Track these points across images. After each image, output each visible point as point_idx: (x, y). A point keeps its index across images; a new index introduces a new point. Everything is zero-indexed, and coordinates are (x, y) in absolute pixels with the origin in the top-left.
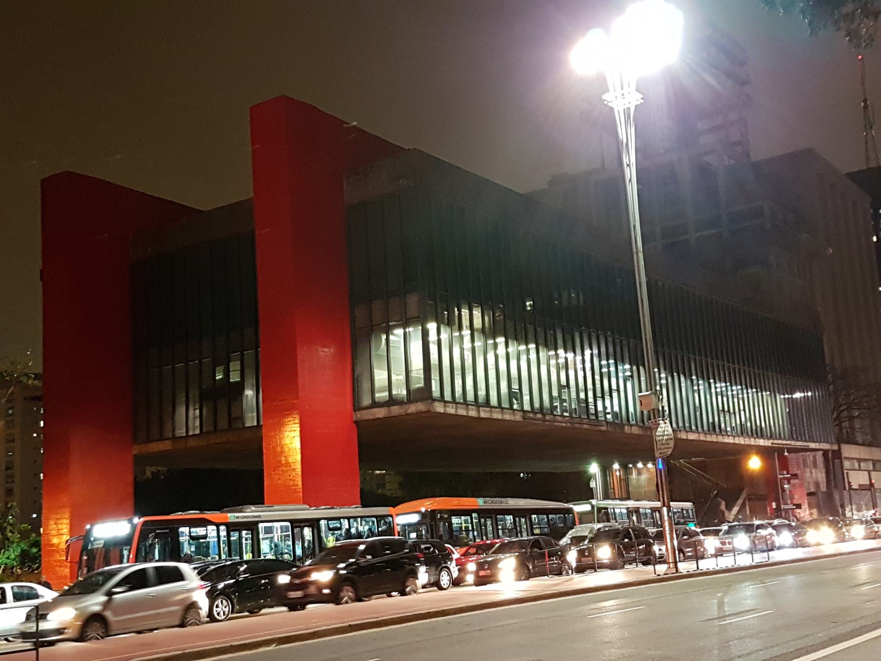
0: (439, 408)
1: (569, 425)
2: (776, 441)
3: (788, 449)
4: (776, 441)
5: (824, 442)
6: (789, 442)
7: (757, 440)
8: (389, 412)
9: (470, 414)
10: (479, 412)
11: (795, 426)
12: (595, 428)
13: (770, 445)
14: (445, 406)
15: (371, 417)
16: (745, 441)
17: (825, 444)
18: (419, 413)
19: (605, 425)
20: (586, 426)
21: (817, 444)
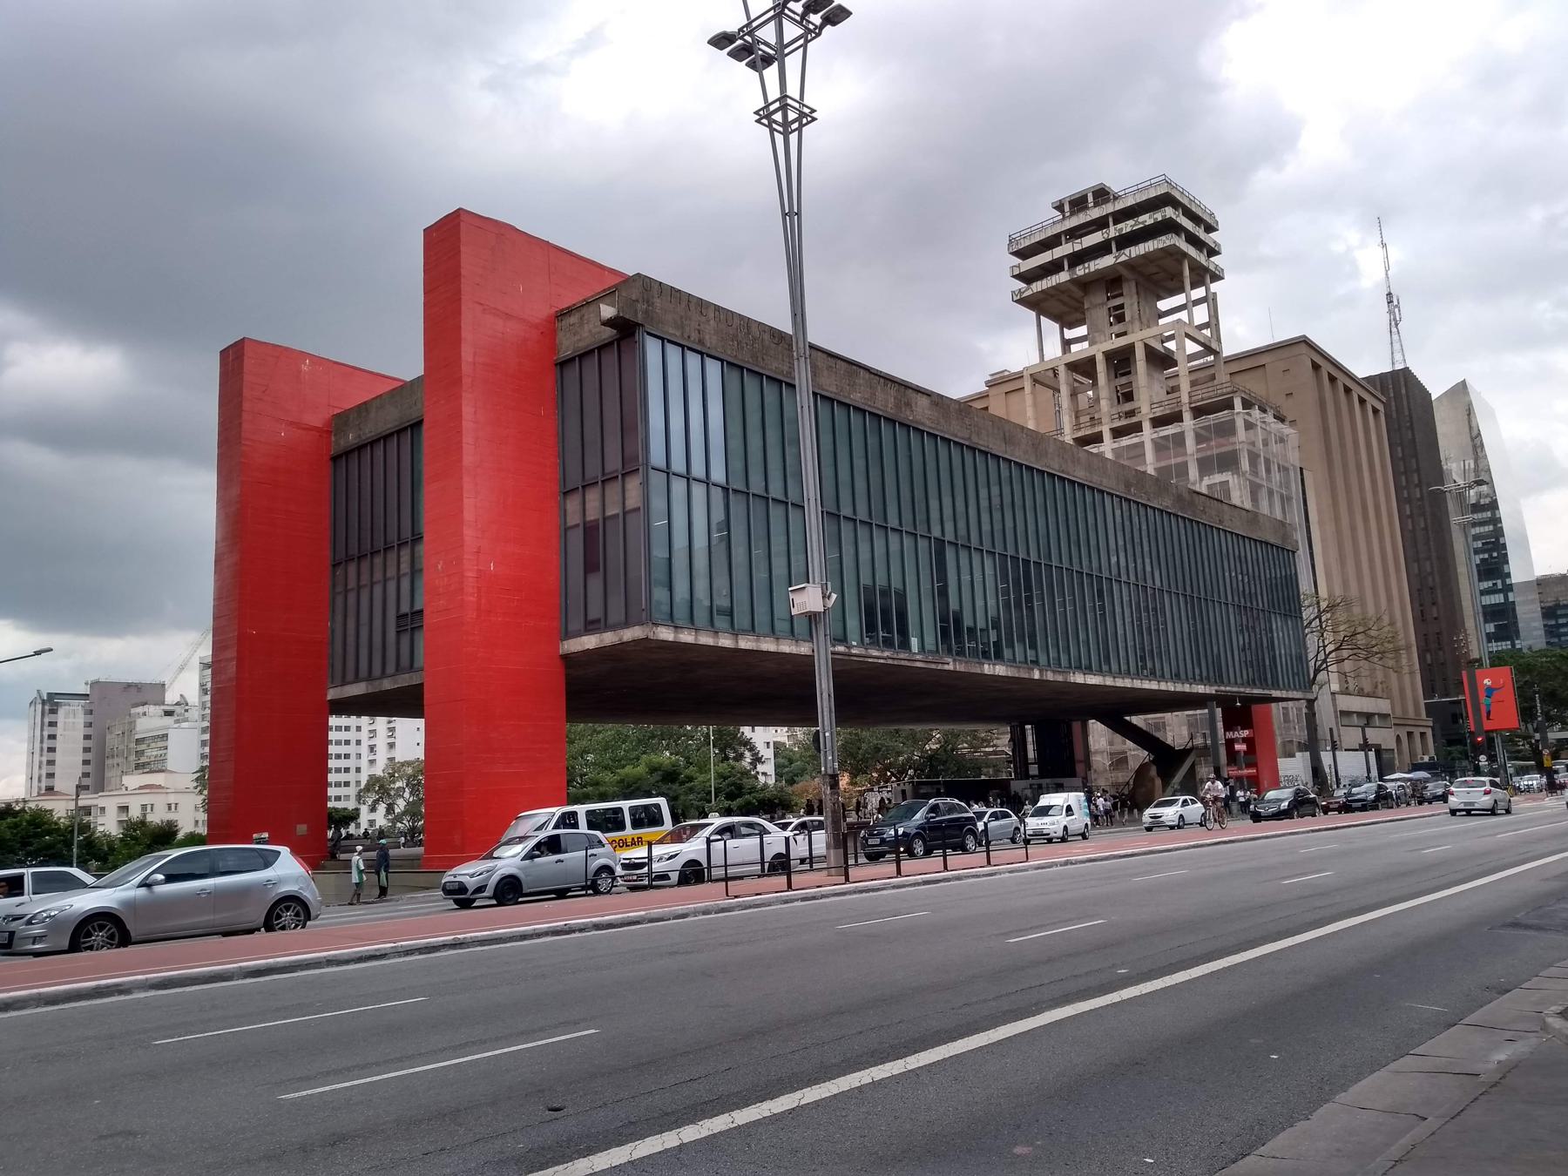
0: (666, 634)
1: (890, 662)
2: (1223, 688)
3: (1240, 697)
4: (1223, 688)
5: (1295, 689)
6: (1242, 690)
7: (1193, 686)
8: (601, 641)
9: (720, 645)
10: (737, 642)
11: (1252, 667)
12: (933, 666)
13: (1214, 692)
14: (676, 632)
15: (580, 648)
16: (1175, 687)
17: (1295, 692)
18: (636, 642)
19: (951, 663)
20: (919, 665)
21: (1284, 692)
